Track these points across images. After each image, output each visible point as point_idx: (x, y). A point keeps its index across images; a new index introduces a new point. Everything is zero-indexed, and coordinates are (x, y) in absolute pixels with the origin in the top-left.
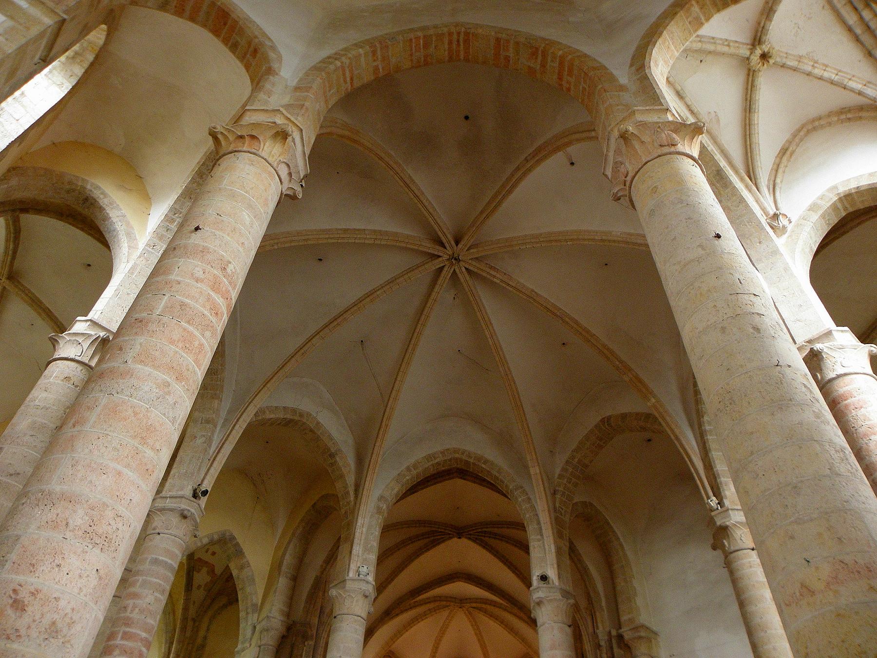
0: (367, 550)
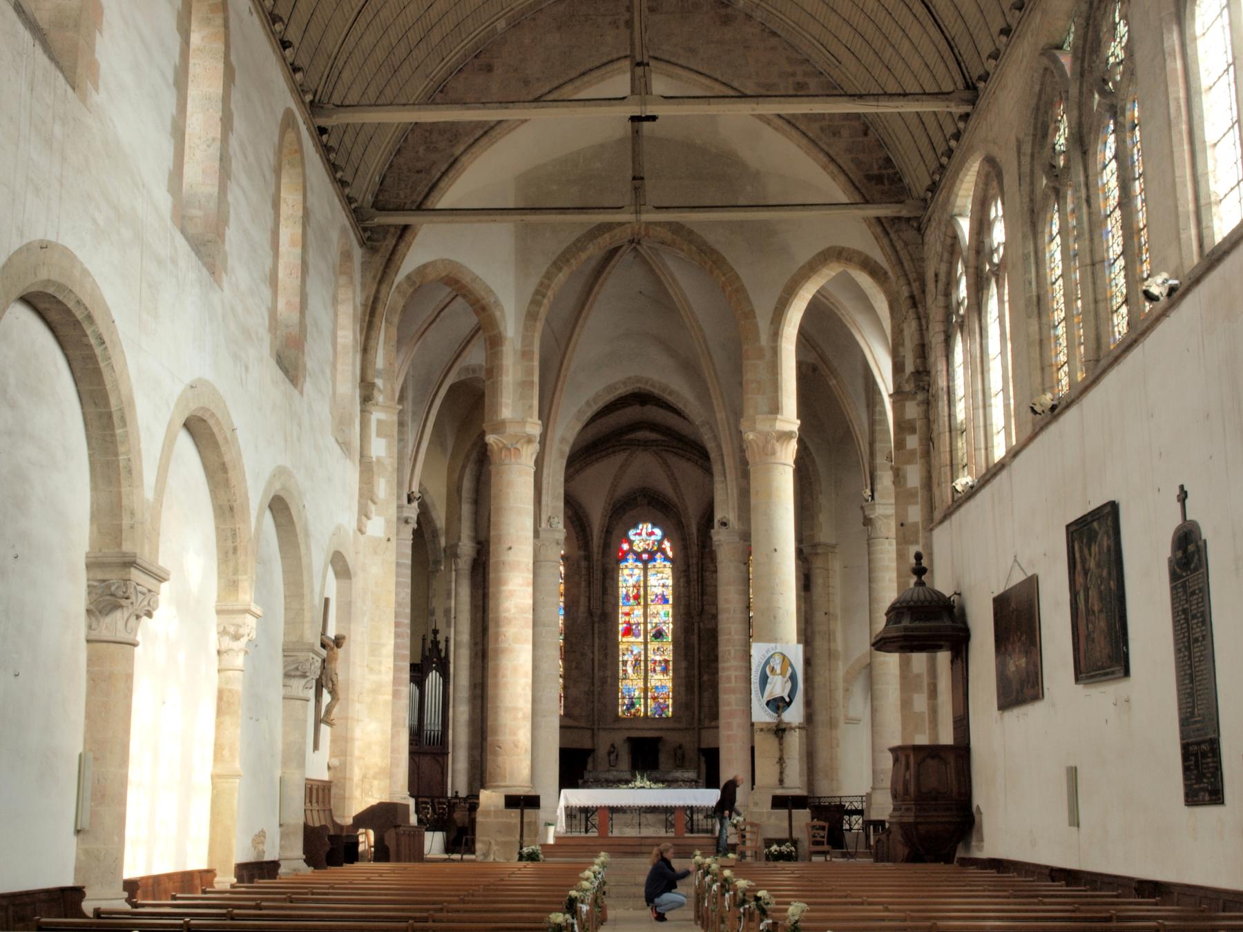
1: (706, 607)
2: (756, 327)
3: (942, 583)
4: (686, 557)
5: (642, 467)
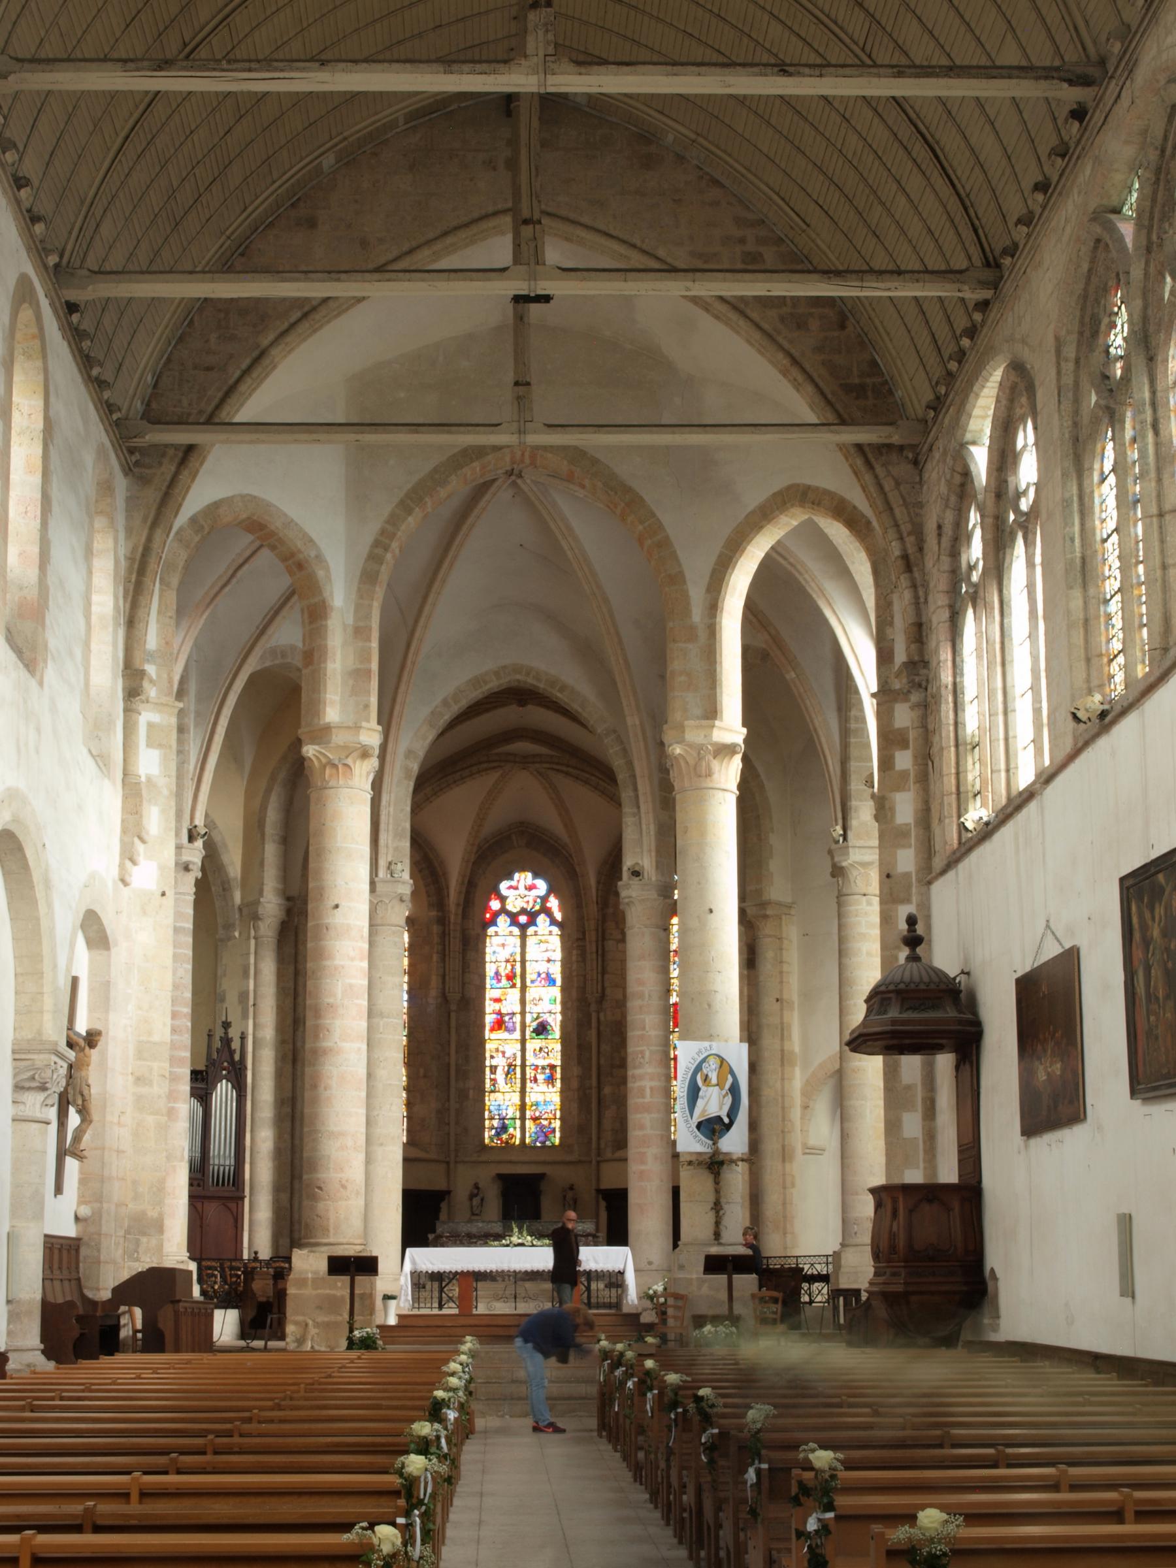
0: (398, 835)
1: (608, 991)
3: (944, 957)
4: (581, 919)
5: (524, 794)
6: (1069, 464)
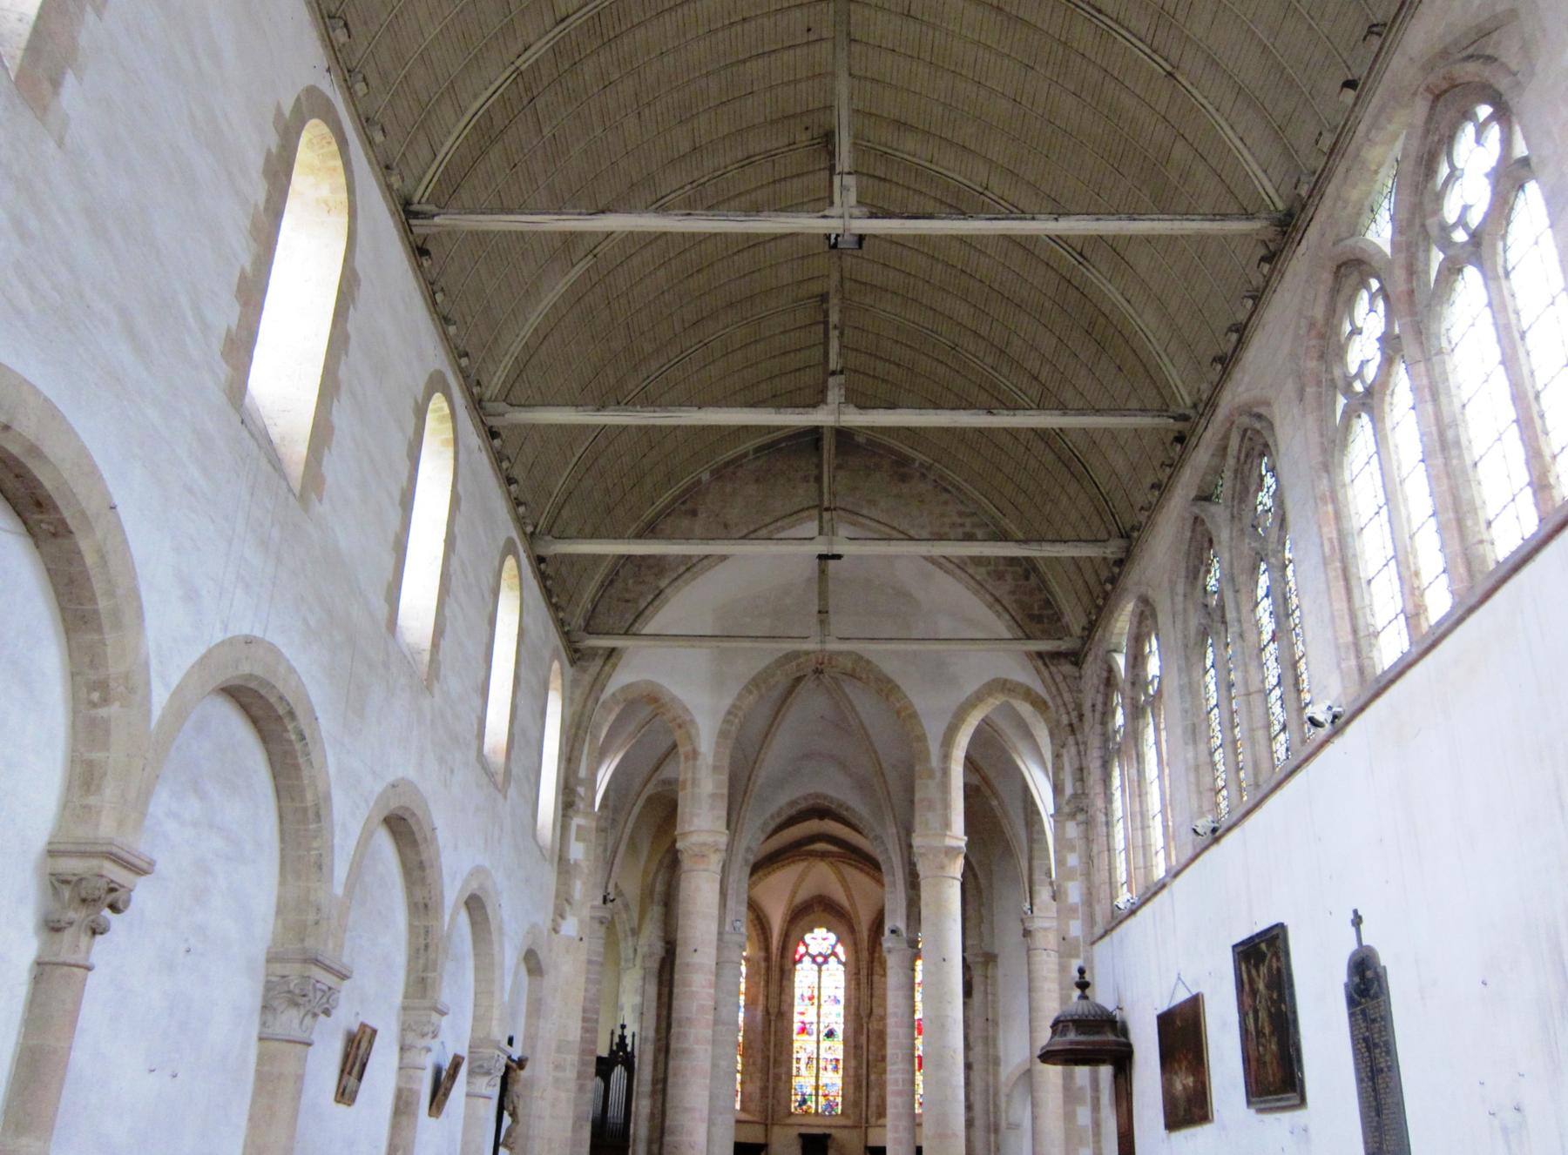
2: (927, 750)
3: (1103, 997)
4: (857, 960)
5: (821, 877)
6: (1182, 662)
